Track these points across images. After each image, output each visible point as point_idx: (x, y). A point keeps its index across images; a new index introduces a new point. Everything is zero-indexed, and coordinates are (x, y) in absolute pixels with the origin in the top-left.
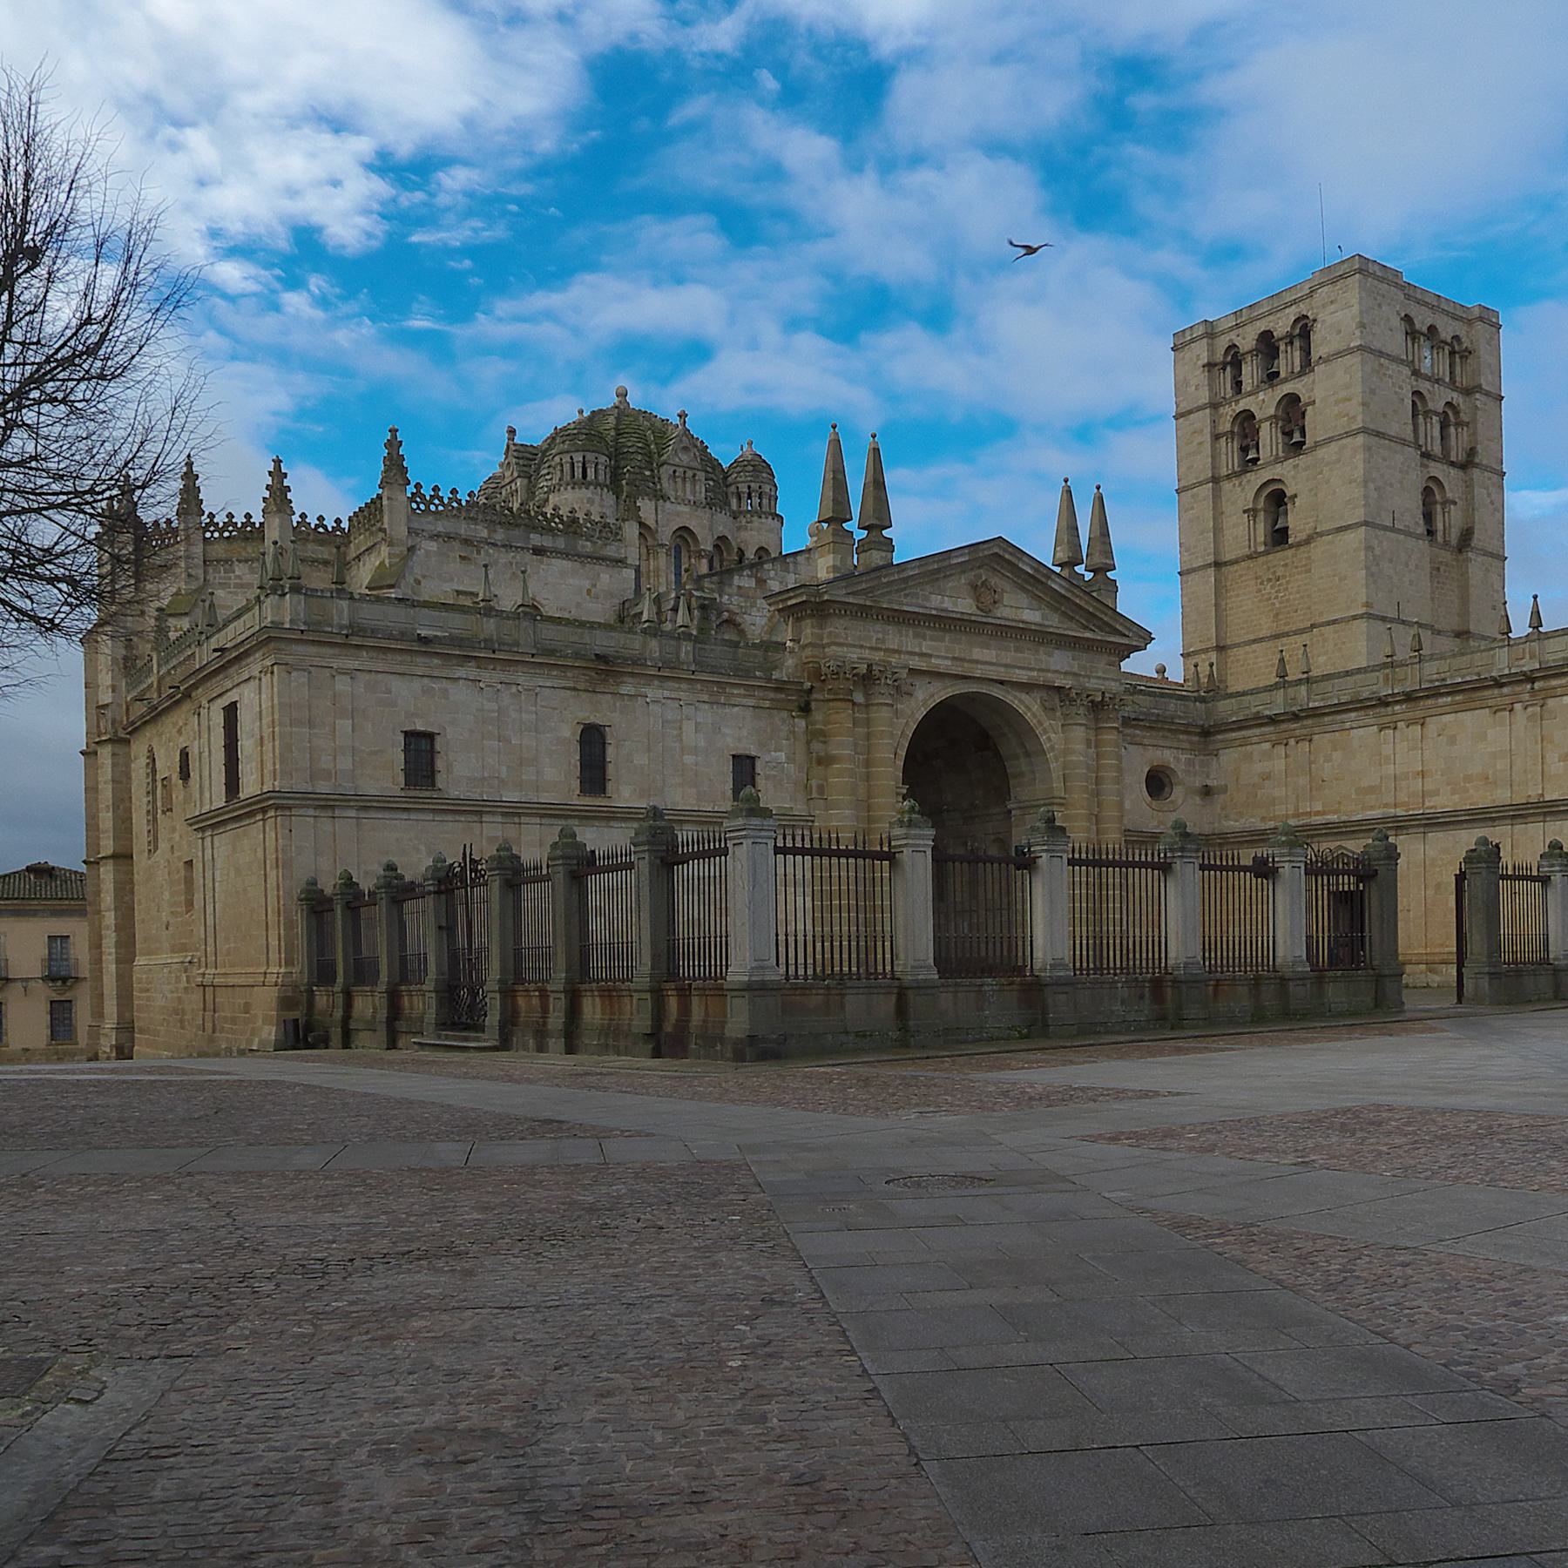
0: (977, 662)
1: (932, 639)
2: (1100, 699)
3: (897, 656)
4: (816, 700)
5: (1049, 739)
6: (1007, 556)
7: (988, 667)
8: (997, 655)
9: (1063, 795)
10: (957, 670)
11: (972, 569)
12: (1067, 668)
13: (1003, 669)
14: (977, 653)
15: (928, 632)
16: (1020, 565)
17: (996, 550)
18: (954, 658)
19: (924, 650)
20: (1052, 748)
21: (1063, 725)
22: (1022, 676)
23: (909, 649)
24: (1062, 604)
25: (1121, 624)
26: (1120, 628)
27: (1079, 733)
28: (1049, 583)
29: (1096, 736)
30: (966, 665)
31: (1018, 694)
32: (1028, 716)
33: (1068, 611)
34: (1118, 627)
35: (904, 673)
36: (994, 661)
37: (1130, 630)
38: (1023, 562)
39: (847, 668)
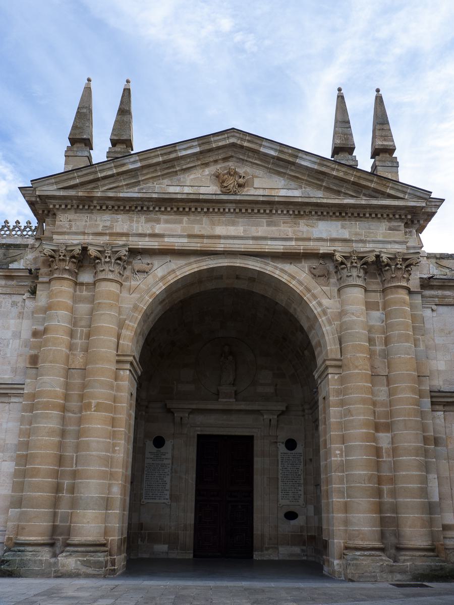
0: (219, 237)
1: (167, 222)
2: (374, 258)
3: (124, 238)
4: (43, 283)
5: (320, 304)
6: (246, 144)
7: (231, 241)
8: (245, 231)
9: (339, 357)
10: (196, 245)
11: (216, 161)
12: (334, 235)
13: (251, 242)
14: (219, 230)
15: (163, 217)
16: (262, 150)
17: (232, 140)
18: (190, 236)
19: (157, 231)
20: (324, 312)
21: (339, 290)
22: (278, 246)
23: (140, 232)
24: (322, 181)
25: (392, 188)
26: (392, 192)
27: (356, 295)
28: (298, 161)
29: (384, 299)
30: (205, 241)
31: (280, 265)
32: (293, 284)
33: (331, 186)
34: (388, 191)
35: (123, 252)
36: (242, 234)
37: (405, 193)
38: (265, 147)
39: (62, 249)
